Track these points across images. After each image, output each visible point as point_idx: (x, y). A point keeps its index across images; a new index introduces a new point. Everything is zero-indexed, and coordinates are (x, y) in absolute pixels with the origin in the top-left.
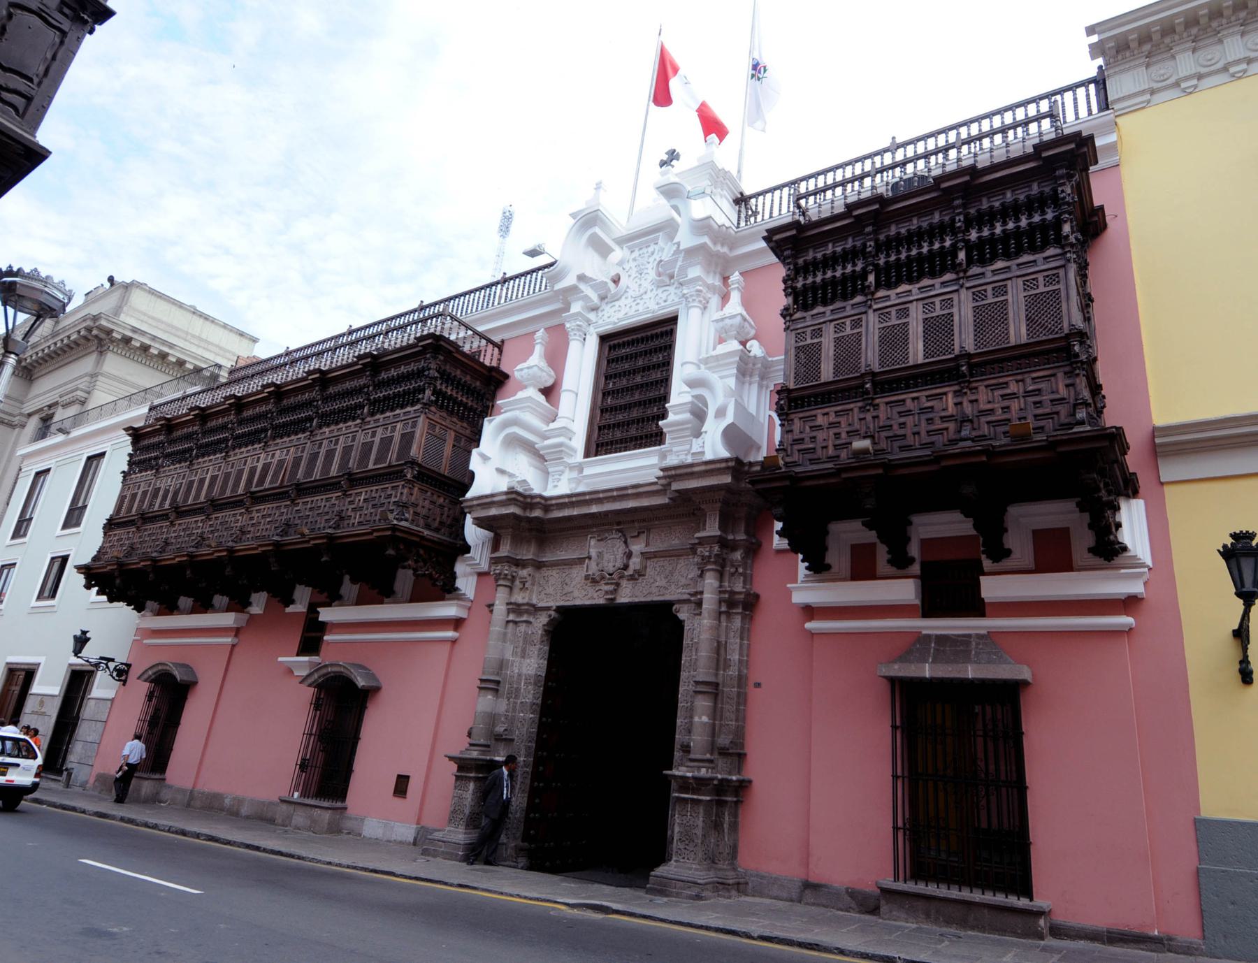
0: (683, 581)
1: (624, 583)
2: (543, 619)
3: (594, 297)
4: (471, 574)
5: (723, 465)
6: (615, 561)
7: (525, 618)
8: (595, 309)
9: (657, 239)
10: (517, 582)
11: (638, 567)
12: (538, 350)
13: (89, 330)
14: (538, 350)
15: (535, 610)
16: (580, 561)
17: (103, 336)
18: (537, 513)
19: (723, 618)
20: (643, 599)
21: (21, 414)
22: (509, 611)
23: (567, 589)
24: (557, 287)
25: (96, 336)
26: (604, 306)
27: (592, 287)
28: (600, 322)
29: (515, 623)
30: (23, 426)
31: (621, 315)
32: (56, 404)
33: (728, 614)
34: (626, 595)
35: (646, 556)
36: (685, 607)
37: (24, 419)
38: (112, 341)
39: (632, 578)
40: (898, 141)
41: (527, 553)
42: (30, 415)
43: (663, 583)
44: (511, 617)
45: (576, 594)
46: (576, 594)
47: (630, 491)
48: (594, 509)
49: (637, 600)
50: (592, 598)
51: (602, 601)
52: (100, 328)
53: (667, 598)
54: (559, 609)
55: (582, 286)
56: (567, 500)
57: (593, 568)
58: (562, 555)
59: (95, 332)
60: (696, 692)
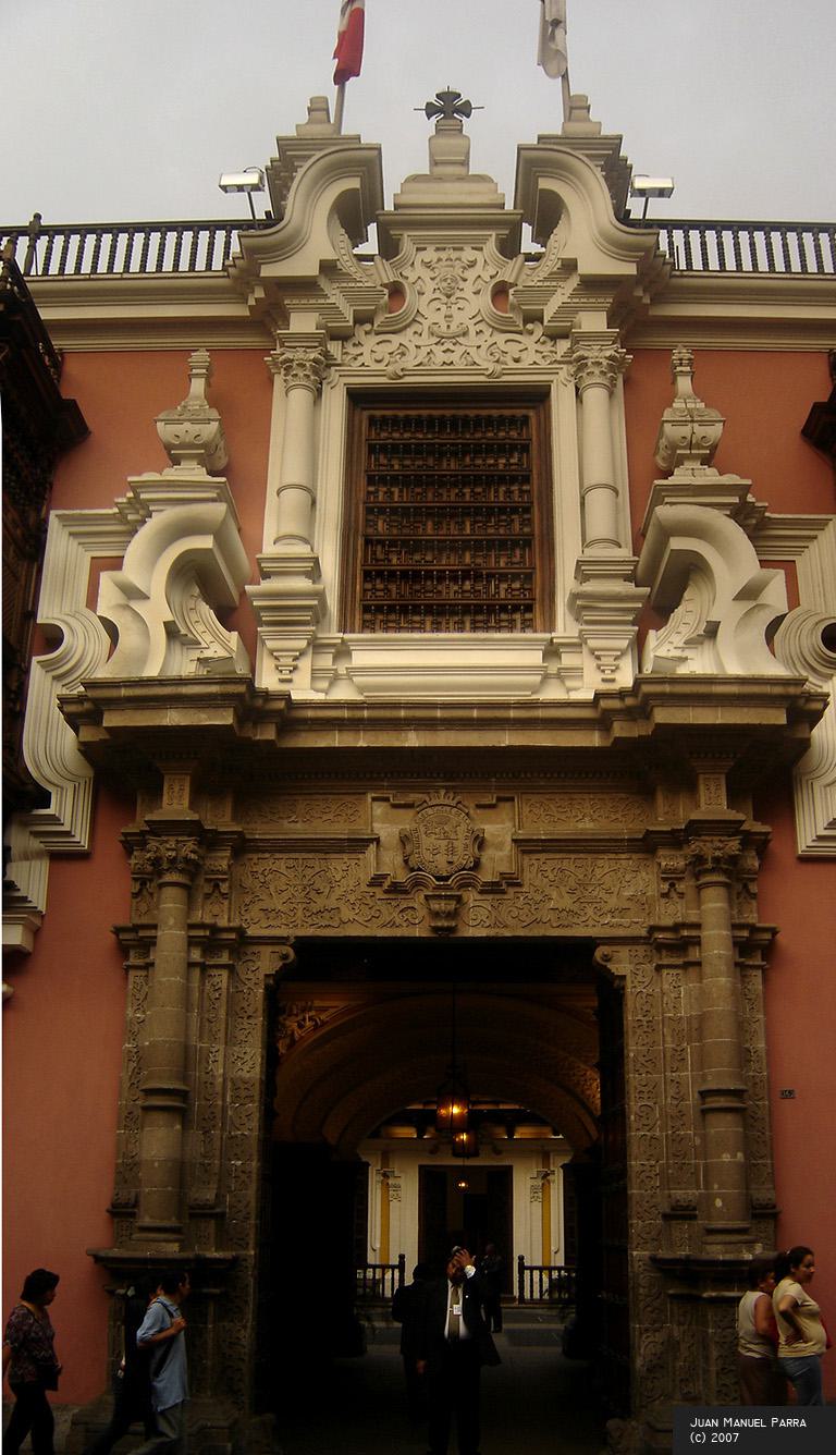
0: (613, 902)
2: (266, 963)
4: (39, 855)
5: (778, 690)
6: (451, 850)
8: (343, 336)
9: (485, 239)
11: (504, 868)
12: (198, 386)
14: (684, 384)
15: (242, 944)
16: (357, 845)
18: (268, 733)
19: (197, 972)
20: (521, 933)
22: (192, 942)
23: (320, 903)
24: (267, 271)
26: (360, 331)
27: (351, 296)
28: (355, 365)
29: (204, 967)
31: (410, 362)
34: (479, 921)
35: (525, 846)
36: (623, 953)
39: (493, 889)
41: (222, 820)
43: (567, 902)
44: (196, 955)
45: (347, 914)
46: (347, 914)
47: (512, 714)
48: (413, 740)
49: (508, 934)
50: (393, 924)
51: (420, 932)
53: (580, 932)
54: (304, 945)
55: (323, 283)
56: (346, 714)
57: (391, 863)
58: (295, 827)
60: (146, 1109)
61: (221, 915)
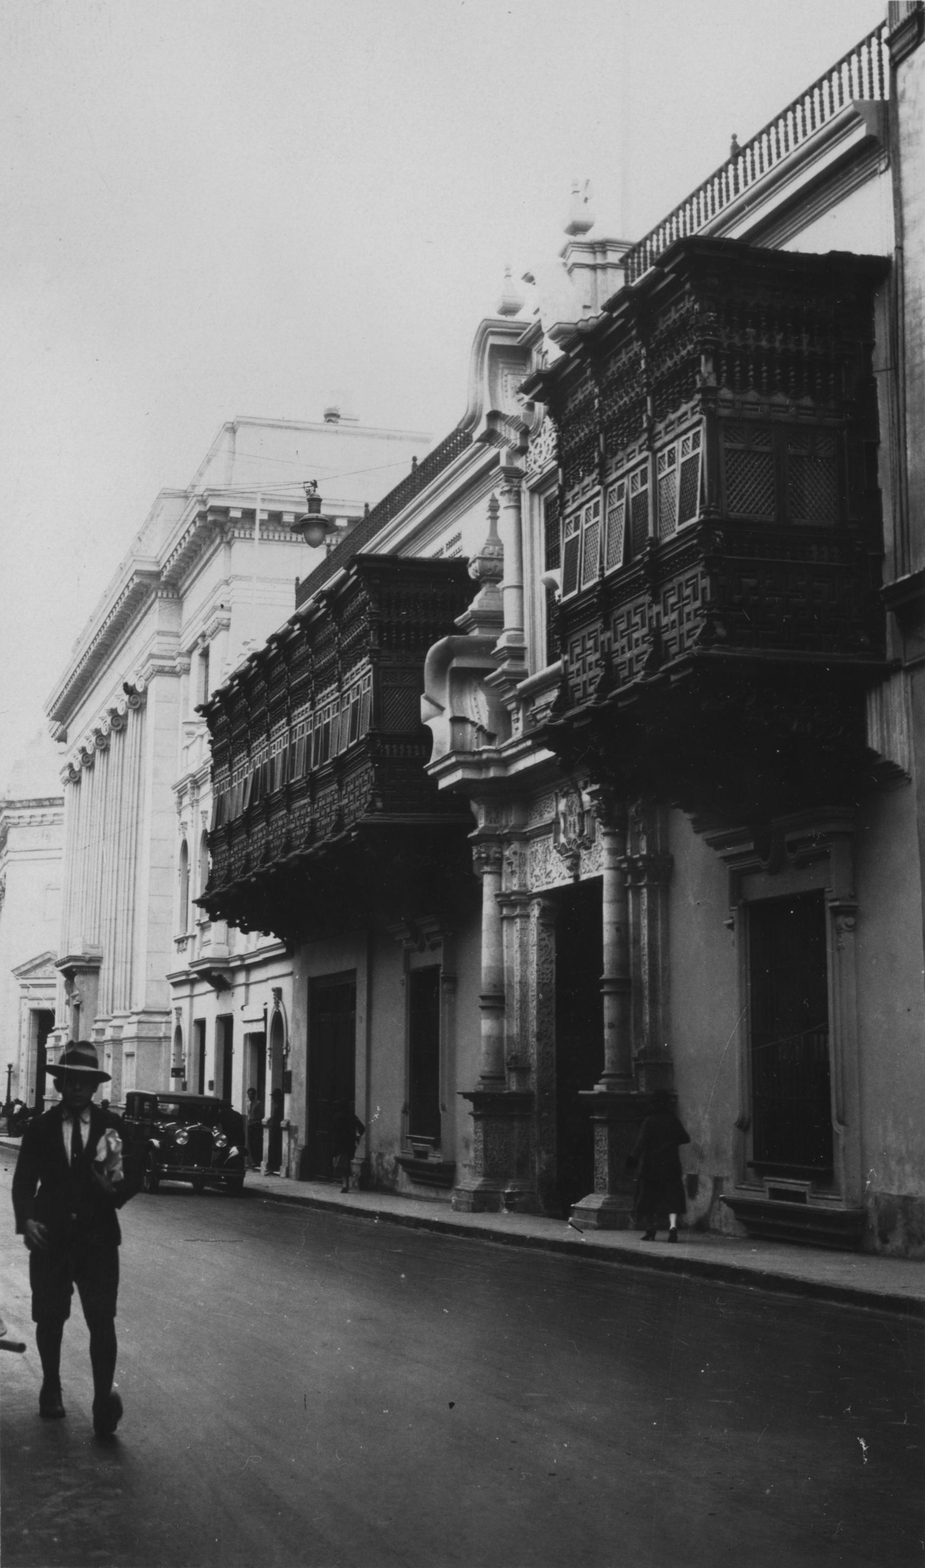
1: (583, 853)
3: (514, 437)
7: (518, 911)
10: (505, 866)
13: (202, 516)
17: (220, 518)
18: (492, 773)
21: (180, 654)
25: (215, 523)
30: (187, 671)
32: (203, 636)
33: (637, 893)
37: (185, 660)
38: (235, 521)
40: (741, 143)
42: (190, 652)
51: (570, 881)
52: (213, 510)
59: (210, 518)
61: (514, 885)
